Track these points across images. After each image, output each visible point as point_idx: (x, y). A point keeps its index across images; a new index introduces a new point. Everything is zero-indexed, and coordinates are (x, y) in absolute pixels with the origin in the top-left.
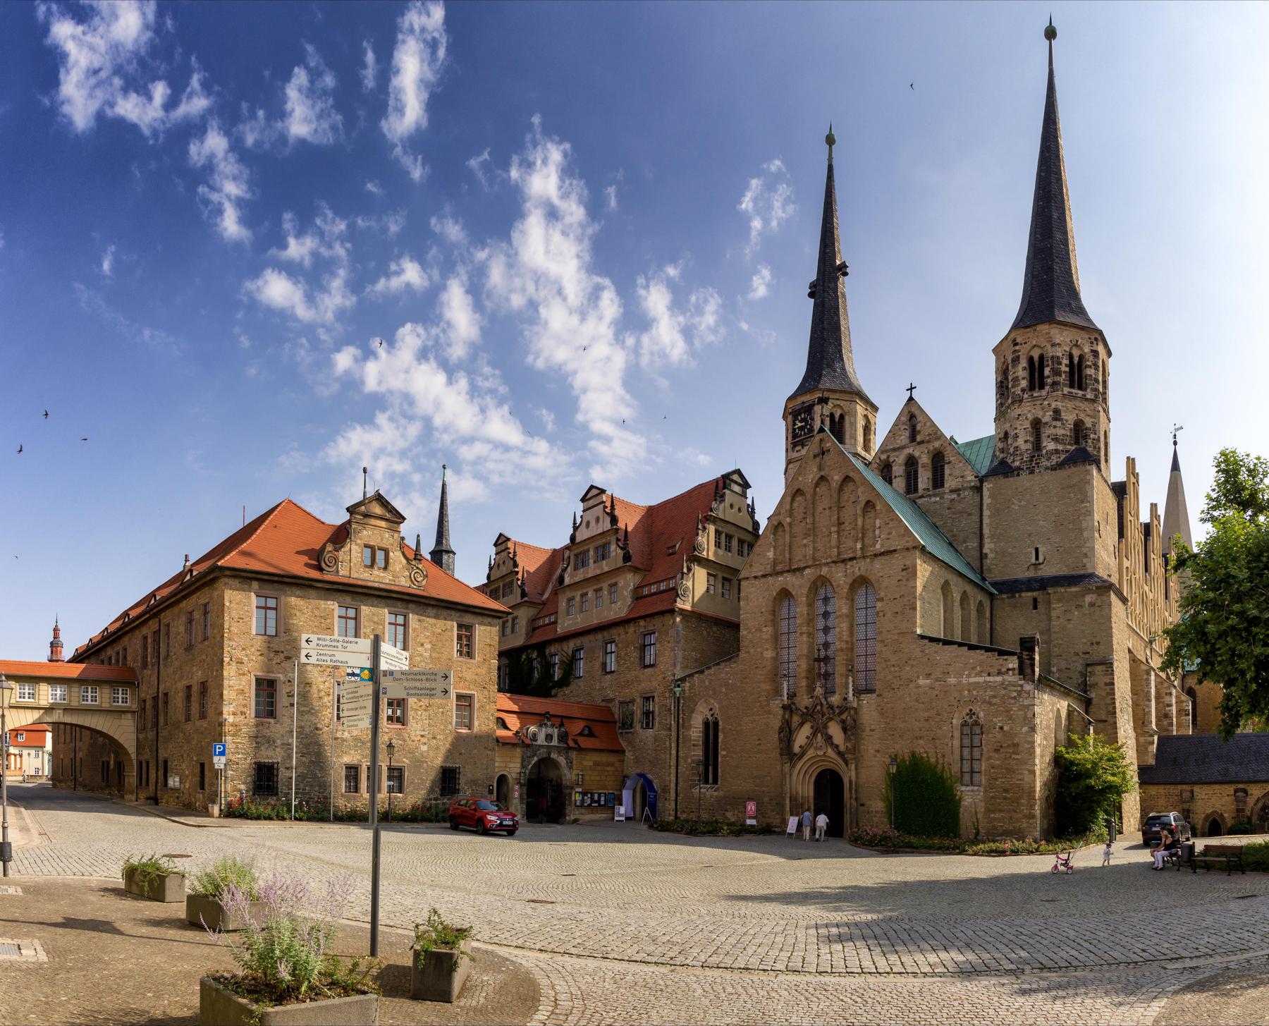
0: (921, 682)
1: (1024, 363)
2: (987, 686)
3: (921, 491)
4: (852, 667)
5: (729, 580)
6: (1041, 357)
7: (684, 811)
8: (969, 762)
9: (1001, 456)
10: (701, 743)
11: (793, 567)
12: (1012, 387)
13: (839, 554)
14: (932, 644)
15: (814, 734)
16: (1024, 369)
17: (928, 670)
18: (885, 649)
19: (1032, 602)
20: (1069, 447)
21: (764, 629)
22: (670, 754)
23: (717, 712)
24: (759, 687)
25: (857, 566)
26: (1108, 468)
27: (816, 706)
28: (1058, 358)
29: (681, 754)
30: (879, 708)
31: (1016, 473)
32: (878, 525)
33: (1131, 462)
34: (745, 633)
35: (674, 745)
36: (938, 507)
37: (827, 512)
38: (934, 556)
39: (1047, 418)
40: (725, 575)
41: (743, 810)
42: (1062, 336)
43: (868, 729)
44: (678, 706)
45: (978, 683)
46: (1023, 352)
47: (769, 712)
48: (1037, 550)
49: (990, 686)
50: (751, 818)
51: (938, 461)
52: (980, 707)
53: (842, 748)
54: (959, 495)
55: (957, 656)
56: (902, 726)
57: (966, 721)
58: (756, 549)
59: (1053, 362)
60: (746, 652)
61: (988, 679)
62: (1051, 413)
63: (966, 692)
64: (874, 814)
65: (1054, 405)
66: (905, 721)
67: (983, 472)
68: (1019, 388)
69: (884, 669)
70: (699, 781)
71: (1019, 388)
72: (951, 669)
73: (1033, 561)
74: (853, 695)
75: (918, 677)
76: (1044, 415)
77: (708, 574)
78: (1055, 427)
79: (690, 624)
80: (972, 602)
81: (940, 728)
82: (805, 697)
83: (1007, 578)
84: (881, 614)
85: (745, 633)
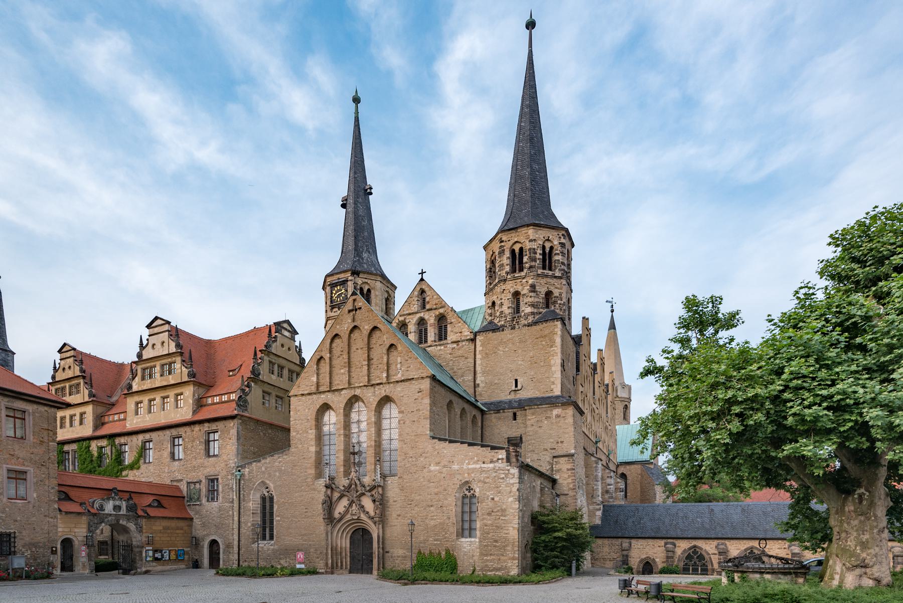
0: (432, 468)
1: (507, 254)
2: (482, 471)
3: (429, 343)
4: (380, 458)
5: (281, 398)
6: (521, 249)
7: (245, 561)
9: (490, 318)
10: (259, 512)
11: (332, 389)
13: (369, 380)
14: (441, 442)
15: (350, 505)
16: (508, 258)
17: (437, 460)
18: (405, 446)
20: (541, 310)
21: (310, 431)
22: (233, 520)
23: (272, 489)
24: (306, 472)
25: (384, 389)
26: (570, 324)
27: (351, 486)
28: (534, 249)
29: (242, 520)
32: (399, 361)
33: (585, 320)
34: (294, 434)
35: (236, 514)
36: (442, 353)
37: (359, 351)
38: (442, 383)
39: (525, 290)
40: (278, 394)
41: (294, 558)
42: (537, 234)
43: (391, 501)
44: (239, 485)
45: (476, 468)
46: (507, 246)
47: (314, 489)
49: (484, 471)
50: (300, 563)
51: (442, 320)
52: (477, 484)
53: (372, 514)
54: (458, 345)
55: (460, 451)
56: (418, 498)
57: (465, 495)
58: (303, 375)
59: (530, 253)
61: (483, 465)
62: (529, 287)
63: (466, 475)
64: (396, 558)
65: (531, 282)
66: (420, 495)
67: (476, 329)
68: (504, 271)
69: (404, 459)
70: (258, 538)
71: (504, 271)
74: (381, 477)
75: (430, 465)
77: (264, 392)
79: (248, 427)
80: (468, 415)
81: (447, 499)
82: (343, 479)
83: (493, 400)
84: (402, 422)
85: (294, 434)
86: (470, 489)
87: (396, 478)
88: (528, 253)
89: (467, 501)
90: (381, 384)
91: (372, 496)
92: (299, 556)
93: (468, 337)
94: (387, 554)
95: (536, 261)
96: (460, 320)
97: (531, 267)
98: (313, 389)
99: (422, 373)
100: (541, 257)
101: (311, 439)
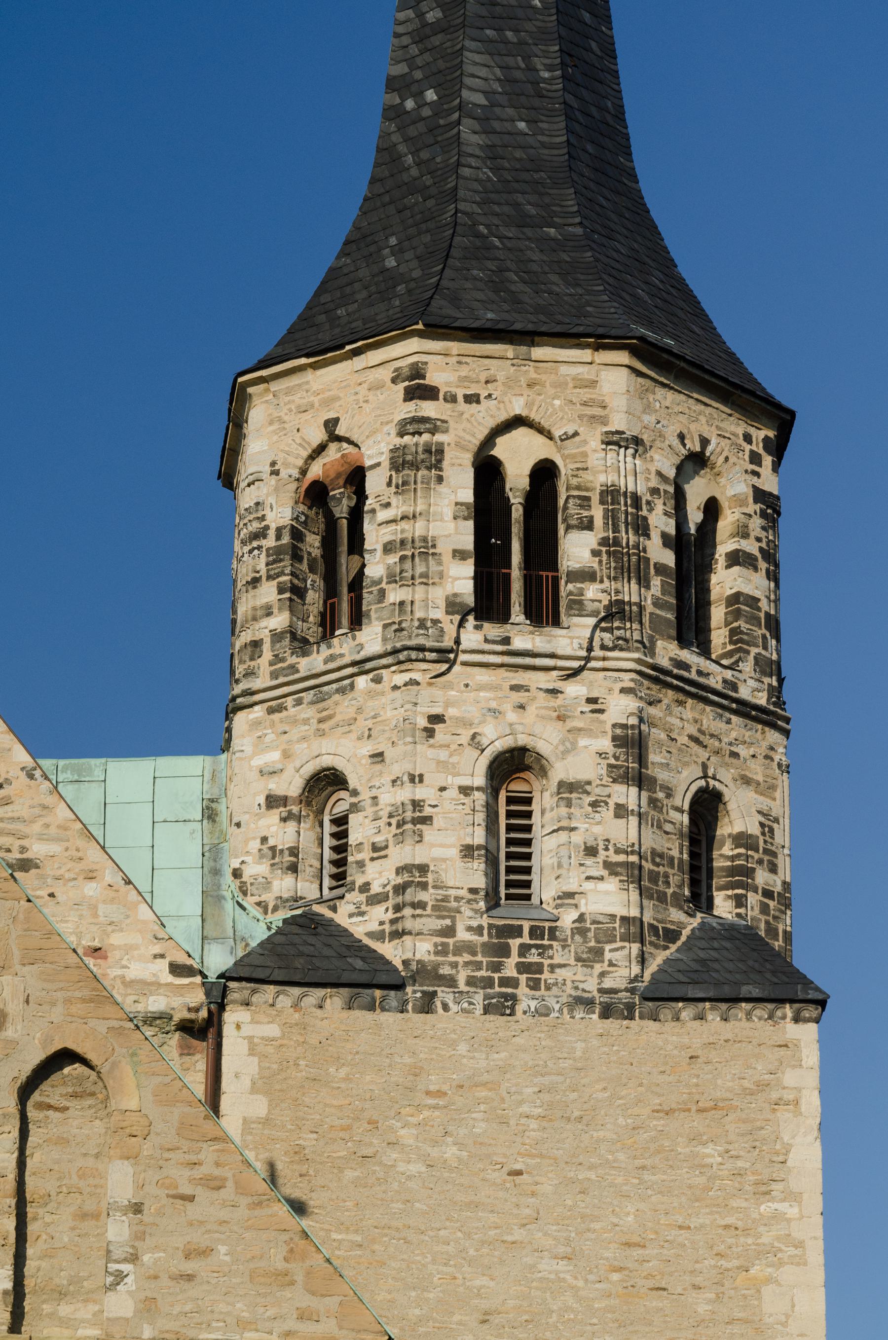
12: (392, 579)
28: (636, 500)
59: (611, 518)
62: (606, 744)
68: (438, 595)
78: (621, 811)
95: (644, 582)
100: (669, 558)
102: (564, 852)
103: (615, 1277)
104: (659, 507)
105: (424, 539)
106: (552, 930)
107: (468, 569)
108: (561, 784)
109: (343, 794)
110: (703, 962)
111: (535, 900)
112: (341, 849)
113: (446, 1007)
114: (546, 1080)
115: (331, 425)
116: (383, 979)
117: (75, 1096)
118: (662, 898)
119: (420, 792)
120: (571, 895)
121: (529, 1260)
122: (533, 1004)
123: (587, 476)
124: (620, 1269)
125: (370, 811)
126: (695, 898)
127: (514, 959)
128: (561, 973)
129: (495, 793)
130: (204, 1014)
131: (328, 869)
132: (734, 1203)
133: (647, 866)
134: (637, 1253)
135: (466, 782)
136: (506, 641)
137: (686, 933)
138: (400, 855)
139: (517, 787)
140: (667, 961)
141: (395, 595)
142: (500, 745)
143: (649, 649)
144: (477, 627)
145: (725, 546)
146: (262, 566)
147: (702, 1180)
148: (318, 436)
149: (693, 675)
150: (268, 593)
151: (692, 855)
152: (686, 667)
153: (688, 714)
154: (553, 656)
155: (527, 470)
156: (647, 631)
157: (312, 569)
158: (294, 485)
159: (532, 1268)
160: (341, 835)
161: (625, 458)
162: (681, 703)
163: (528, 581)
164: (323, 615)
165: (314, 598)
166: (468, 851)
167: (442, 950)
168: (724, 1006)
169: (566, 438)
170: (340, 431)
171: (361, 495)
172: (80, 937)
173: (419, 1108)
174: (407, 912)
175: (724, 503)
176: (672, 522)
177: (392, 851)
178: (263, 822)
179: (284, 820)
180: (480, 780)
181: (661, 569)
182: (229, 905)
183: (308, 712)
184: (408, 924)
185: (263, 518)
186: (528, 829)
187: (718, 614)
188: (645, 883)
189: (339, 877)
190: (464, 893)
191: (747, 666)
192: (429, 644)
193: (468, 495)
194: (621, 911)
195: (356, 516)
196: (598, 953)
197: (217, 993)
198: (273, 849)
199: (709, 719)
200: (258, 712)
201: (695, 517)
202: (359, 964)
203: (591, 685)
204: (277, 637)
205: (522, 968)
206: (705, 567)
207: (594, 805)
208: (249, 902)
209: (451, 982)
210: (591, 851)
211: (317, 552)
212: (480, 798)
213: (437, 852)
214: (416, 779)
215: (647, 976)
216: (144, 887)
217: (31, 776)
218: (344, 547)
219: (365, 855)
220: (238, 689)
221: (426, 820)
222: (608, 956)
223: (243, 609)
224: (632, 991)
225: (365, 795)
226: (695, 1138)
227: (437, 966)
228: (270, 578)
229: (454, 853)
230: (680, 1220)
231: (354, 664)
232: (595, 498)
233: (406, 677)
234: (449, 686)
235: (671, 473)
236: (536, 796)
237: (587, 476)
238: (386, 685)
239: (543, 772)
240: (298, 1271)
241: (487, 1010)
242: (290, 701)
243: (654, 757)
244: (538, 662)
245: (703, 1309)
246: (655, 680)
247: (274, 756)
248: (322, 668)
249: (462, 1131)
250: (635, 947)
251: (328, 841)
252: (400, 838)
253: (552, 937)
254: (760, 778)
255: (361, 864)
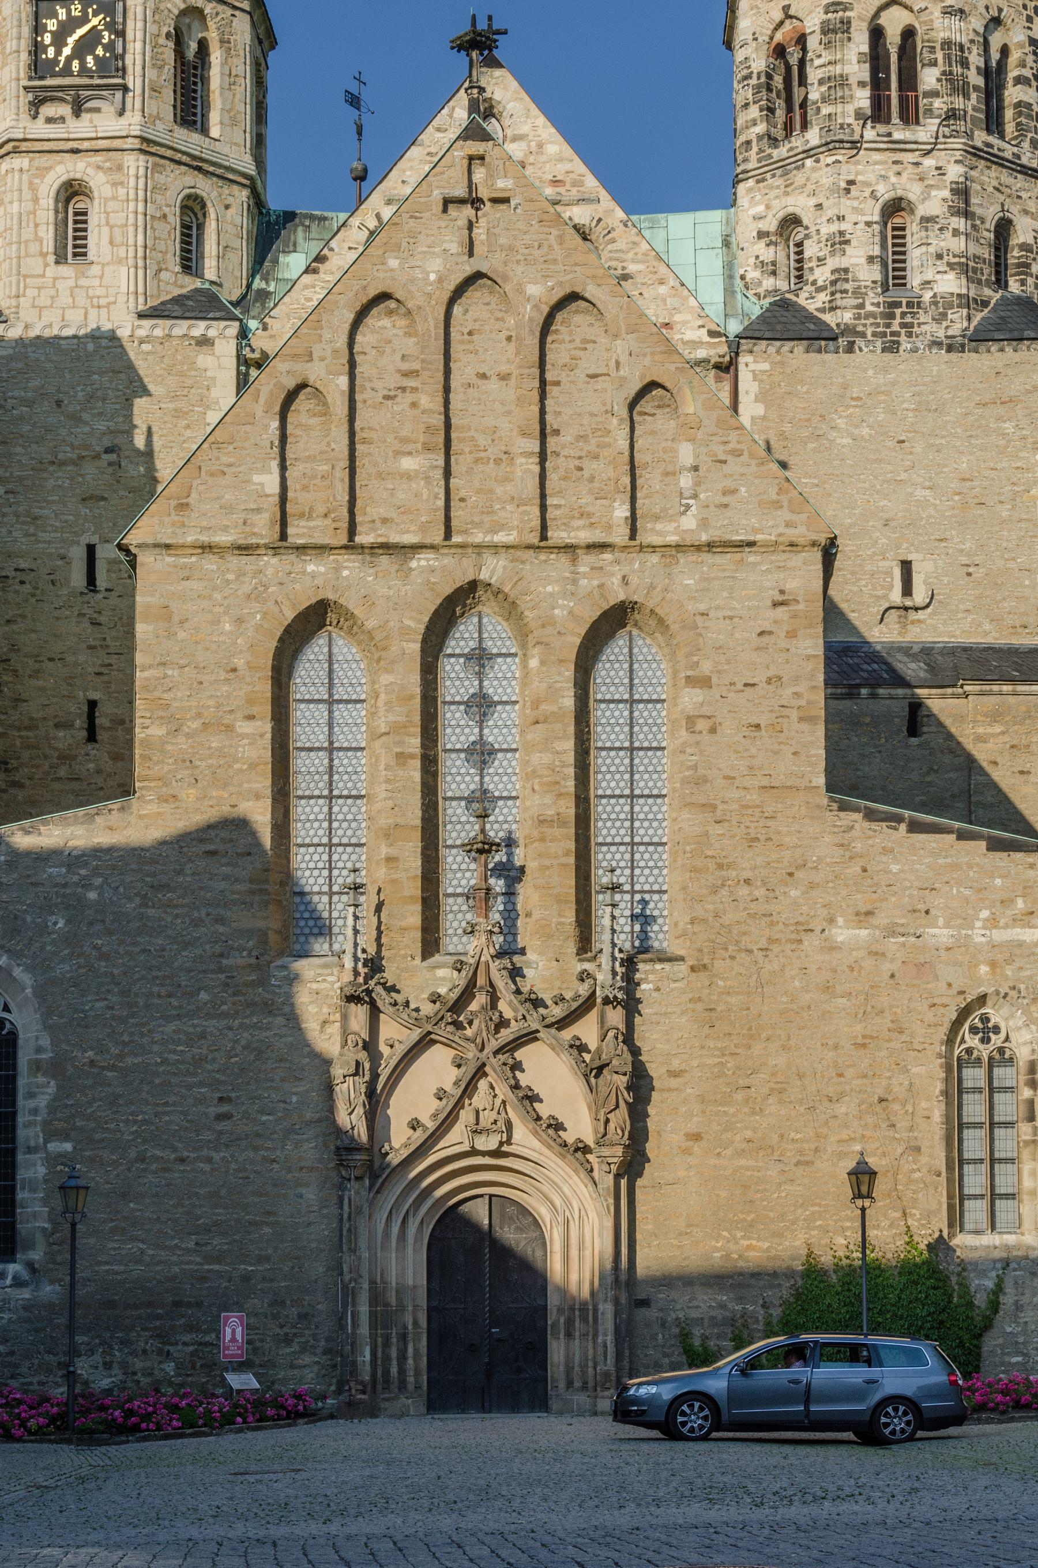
1: (861, 43)
6: (909, 33)
8: (984, 1168)
12: (824, 100)
19: (906, 713)
21: (245, 727)
24: (220, 920)
28: (962, 48)
30: (700, 1007)
31: (842, 342)
34: (157, 731)
48: (906, 566)
56: (780, 1061)
60: (163, 799)
62: (946, 193)
68: (850, 109)
69: (714, 890)
71: (850, 109)
72: (936, 902)
73: (896, 596)
76: (926, 198)
78: (956, 233)
84: (702, 725)
85: (157, 731)
86: (986, 1031)
87: (682, 968)
88: (940, 55)
89: (975, 1077)
90: (602, 547)
91: (581, 1048)
92: (228, 1330)
93: (701, 354)
94: (642, 1313)
95: (966, 96)
96: (663, 270)
97: (952, 115)
98: (264, 529)
99: (788, 525)
100: (980, 82)
101: (253, 766)
102: (924, 258)
103: (957, 498)
104: (975, 51)
105: (841, 76)
106: (919, 303)
107: (866, 93)
108: (922, 218)
109: (800, 229)
110: (1002, 318)
111: (909, 286)
112: (799, 261)
113: (861, 350)
114: (917, 389)
115: (786, 8)
116: (825, 334)
117: (659, 407)
118: (979, 282)
119: (844, 226)
120: (928, 282)
121: (909, 490)
122: (909, 346)
123: (933, 34)
124: (959, 494)
125: (815, 238)
126: (998, 281)
127: (898, 321)
128: (924, 328)
129: (885, 224)
130: (727, 358)
131: (794, 273)
132: (1021, 455)
133: (971, 264)
134: (968, 484)
135: (869, 219)
136: (889, 135)
137: (993, 302)
138: (833, 263)
139: (897, 221)
140: (983, 319)
141: (826, 110)
142: (887, 197)
143: (970, 136)
144: (873, 127)
145: (1012, 73)
146: (750, 96)
147: (1003, 442)
148: (778, 15)
149: (995, 151)
150: (754, 112)
151: (997, 257)
152: (991, 146)
153: (993, 174)
154: (916, 143)
155: (899, 32)
156: (969, 125)
157: (778, 97)
158: (766, 47)
159: (911, 494)
160: (800, 253)
161: (955, 22)
162: (989, 168)
163: (900, 97)
164: (785, 124)
165: (780, 114)
166: (871, 259)
167: (858, 317)
168: (1014, 343)
169: (921, 11)
170: (792, 12)
171: (804, 50)
172: (657, 316)
173: (847, 407)
174: (838, 295)
175: (1012, 47)
176: (982, 59)
177: (829, 261)
178: (756, 247)
179: (768, 245)
180: (876, 218)
181: (976, 88)
182: (739, 296)
183: (779, 182)
184: (839, 303)
185: (749, 67)
186: (904, 245)
187: (1009, 114)
188: (970, 274)
189: (799, 277)
190: (868, 283)
191: (1026, 145)
192: (846, 138)
193: (865, 48)
194: (957, 291)
195: (802, 63)
196: (944, 315)
197: (734, 346)
198: (762, 262)
199: (1005, 177)
200: (751, 183)
201: (995, 56)
202: (812, 327)
203: (937, 159)
204: (760, 138)
205: (903, 325)
206: (1001, 87)
207: (941, 229)
208: (750, 293)
209: (863, 335)
210: (940, 257)
211: (781, 86)
212: (877, 228)
213: (854, 261)
214: (841, 218)
215: (972, 328)
216: (692, 287)
217: (626, 226)
218: (796, 83)
219: (813, 264)
220: (739, 170)
221: (847, 242)
222: (950, 317)
223: (740, 122)
224: (964, 336)
225: (813, 229)
226: (1000, 419)
227: (855, 326)
228: (754, 102)
229: (863, 260)
230: (992, 465)
231: (804, 152)
232: (938, 47)
233: (834, 158)
234: (858, 163)
235: (981, 30)
236: (908, 225)
237: (933, 34)
238: (822, 163)
239: (912, 212)
240: (784, 500)
241: (883, 350)
242: (768, 175)
243: (974, 200)
244: (908, 146)
245: (1005, 514)
246: (975, 155)
247: (760, 209)
248: (786, 155)
249: (871, 419)
250: (965, 311)
251: (793, 257)
252: (833, 253)
253: (919, 307)
254: (1034, 210)
255: (811, 269)
